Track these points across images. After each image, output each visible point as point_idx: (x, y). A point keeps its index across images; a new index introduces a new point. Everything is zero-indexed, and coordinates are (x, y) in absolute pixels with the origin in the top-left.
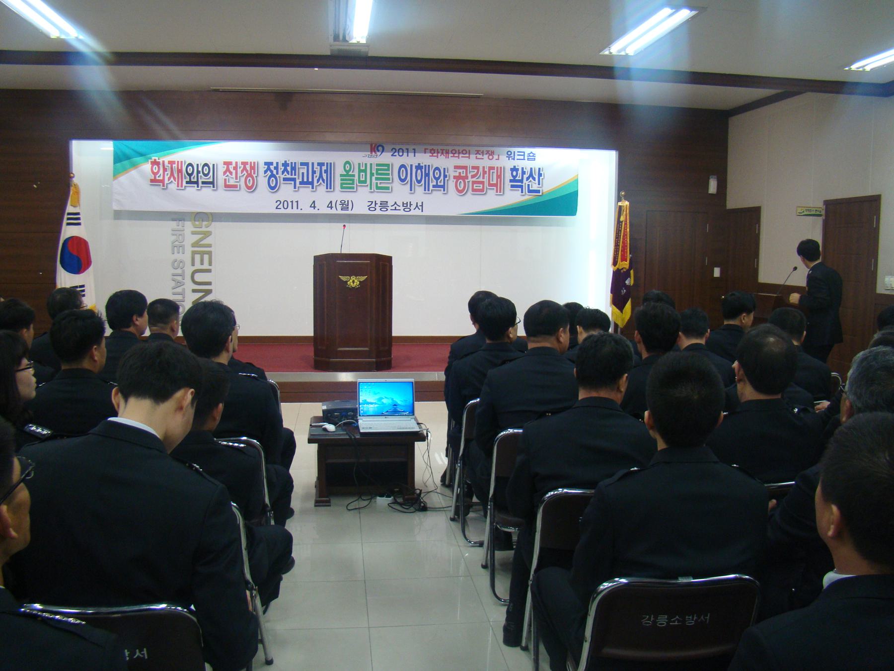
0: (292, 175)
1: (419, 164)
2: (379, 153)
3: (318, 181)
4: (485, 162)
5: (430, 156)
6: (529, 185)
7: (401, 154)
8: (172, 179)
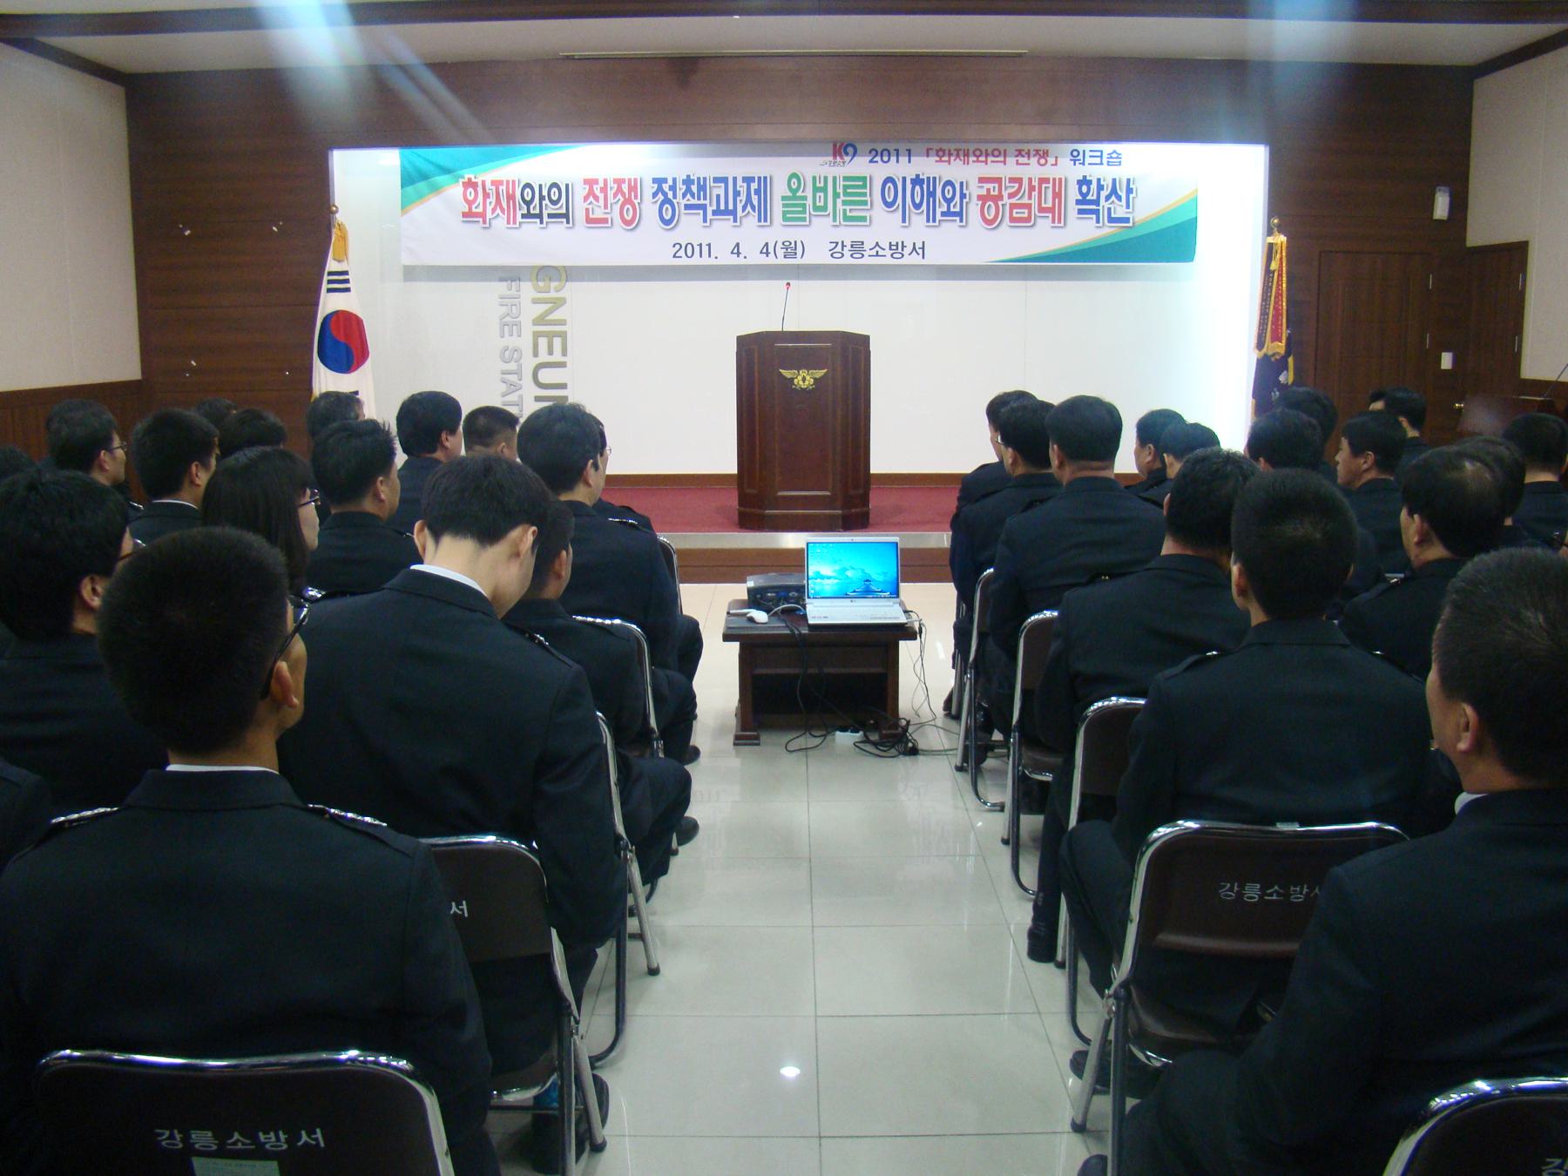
0: (699, 199)
1: (918, 176)
2: (847, 159)
3: (744, 208)
4: (1032, 170)
5: (937, 161)
6: (1109, 209)
7: (885, 159)
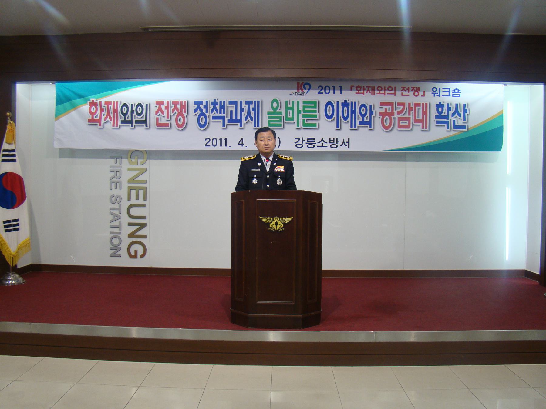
0: (220, 113)
1: (345, 101)
2: (305, 91)
3: (246, 118)
4: (410, 99)
5: (356, 93)
6: (454, 121)
7: (327, 91)
8: (108, 119)
